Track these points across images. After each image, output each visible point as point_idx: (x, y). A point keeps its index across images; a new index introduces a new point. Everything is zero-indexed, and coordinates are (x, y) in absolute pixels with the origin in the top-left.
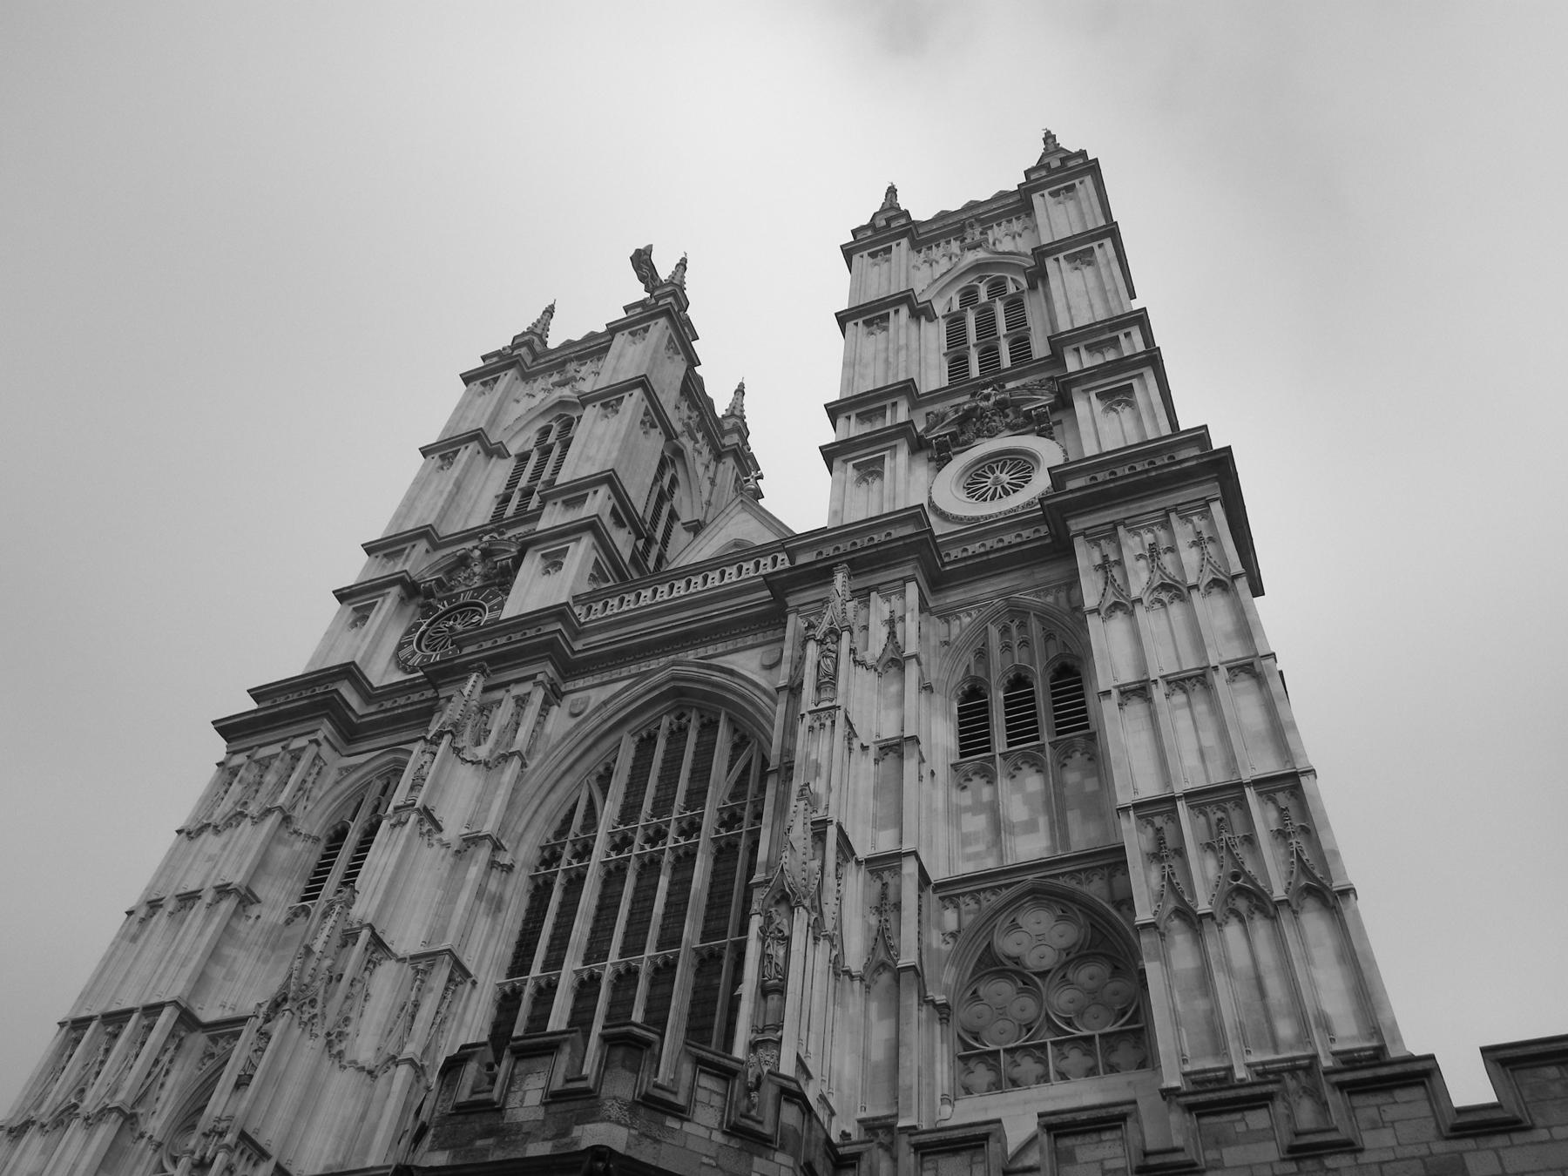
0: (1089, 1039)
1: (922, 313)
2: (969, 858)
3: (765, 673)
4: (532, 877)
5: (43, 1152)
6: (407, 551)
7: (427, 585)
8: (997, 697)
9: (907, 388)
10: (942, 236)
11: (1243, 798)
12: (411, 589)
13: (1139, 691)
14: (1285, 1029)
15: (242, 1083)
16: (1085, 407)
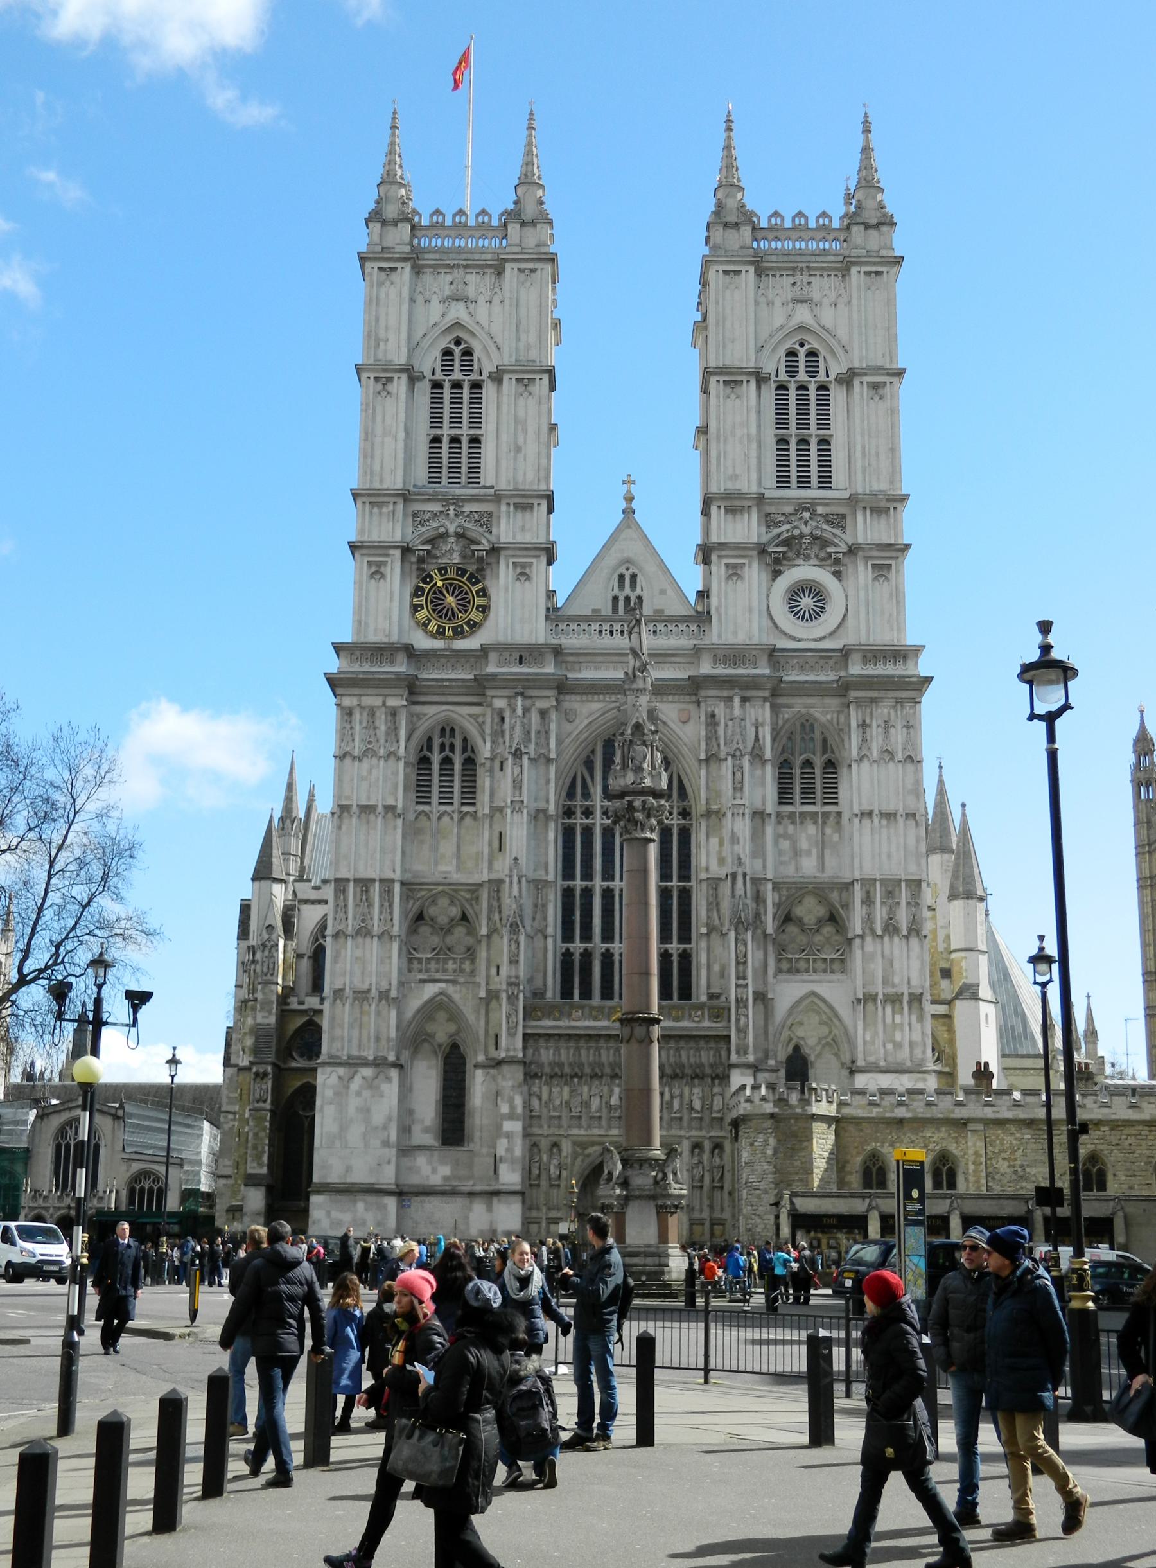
0: (825, 960)
1: (760, 378)
2: (782, 863)
3: (681, 724)
4: (563, 824)
5: (357, 947)
6: (391, 507)
7: (421, 553)
8: (797, 772)
9: (761, 499)
10: (779, 268)
11: (900, 886)
12: (406, 550)
13: (870, 814)
14: (897, 980)
15: (514, 961)
16: (862, 573)
